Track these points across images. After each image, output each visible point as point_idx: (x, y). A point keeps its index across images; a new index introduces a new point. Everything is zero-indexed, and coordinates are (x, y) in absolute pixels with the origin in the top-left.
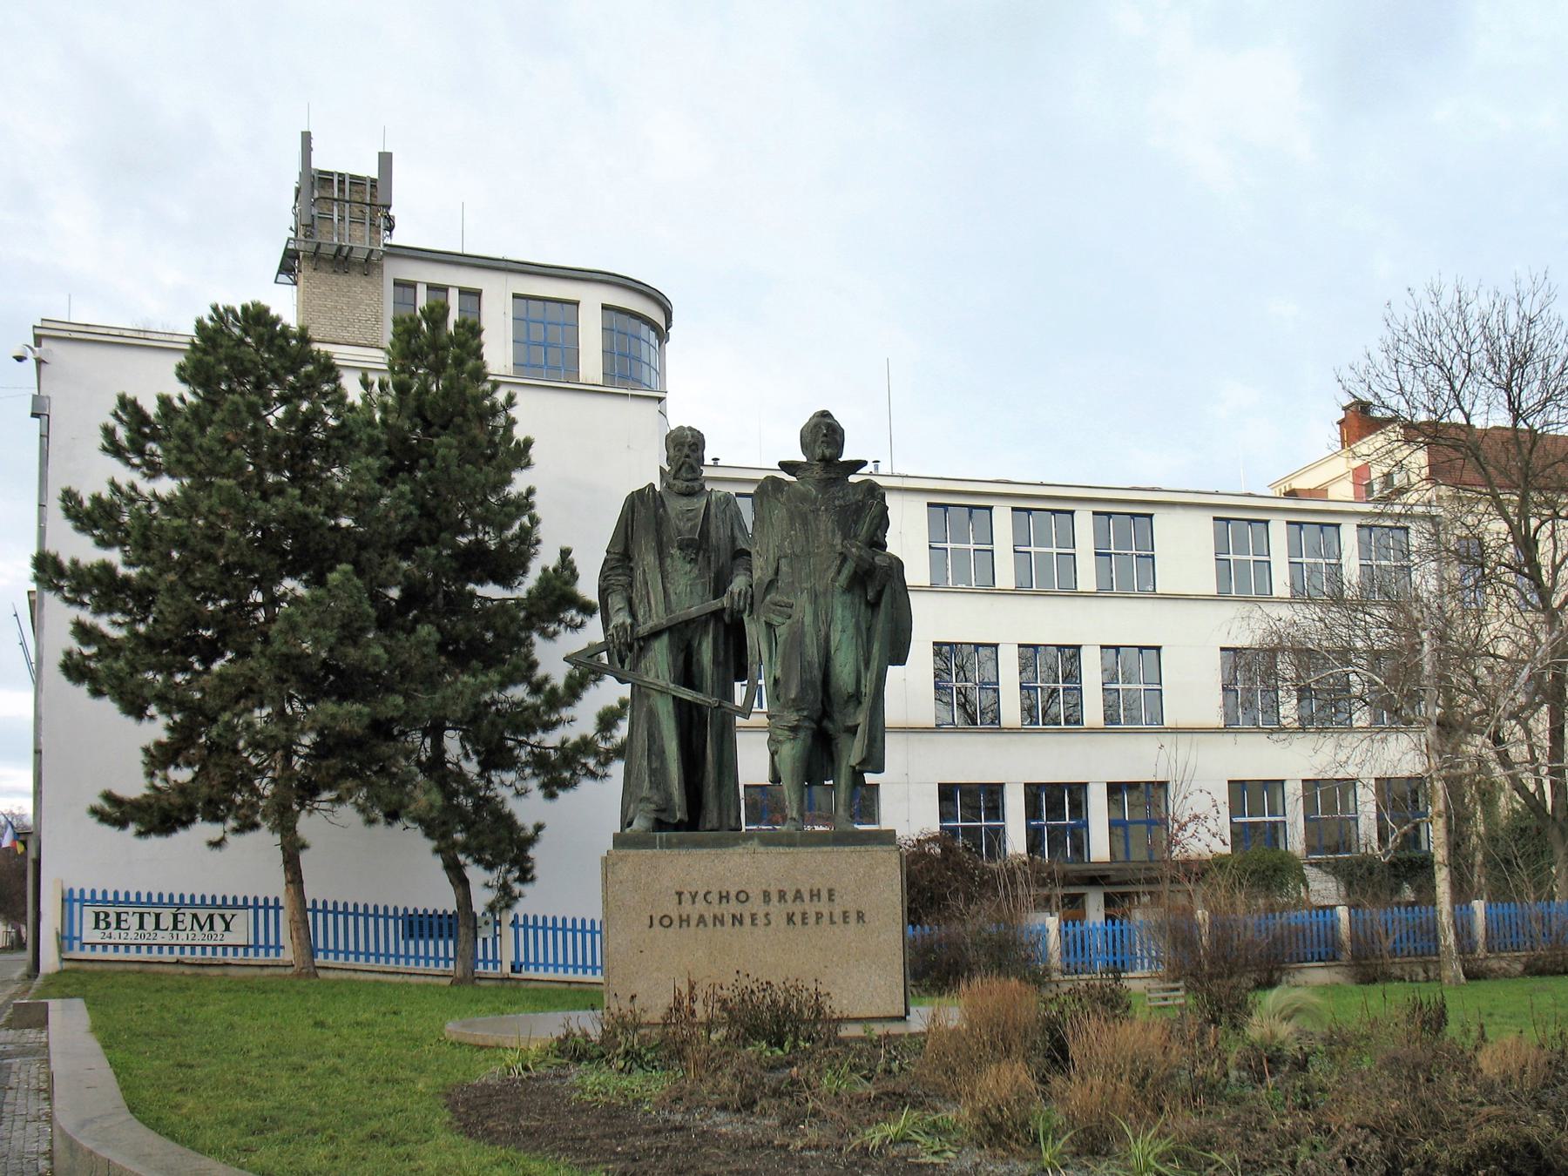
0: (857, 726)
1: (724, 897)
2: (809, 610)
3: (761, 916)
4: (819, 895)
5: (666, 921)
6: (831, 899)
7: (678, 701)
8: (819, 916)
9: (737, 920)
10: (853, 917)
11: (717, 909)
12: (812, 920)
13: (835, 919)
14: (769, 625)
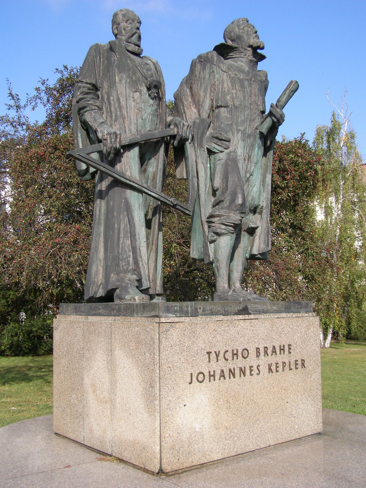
0: (257, 228)
2: (241, 144)
3: (255, 368)
4: (283, 350)
6: (290, 353)
9: (242, 371)
10: (299, 363)
11: (231, 365)
12: (280, 369)
13: (292, 367)
14: (210, 152)
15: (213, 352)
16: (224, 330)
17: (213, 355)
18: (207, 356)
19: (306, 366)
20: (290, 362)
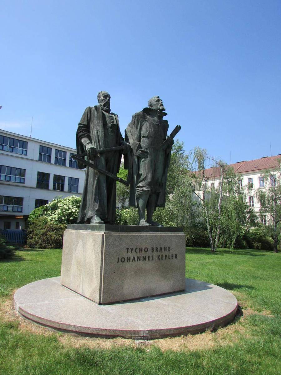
0: (160, 192)
1: (141, 250)
3: (151, 257)
5: (123, 260)
6: (169, 251)
7: (107, 178)
8: (166, 256)
10: (174, 256)
11: (139, 255)
12: (164, 258)
15: (130, 248)
16: (136, 239)
17: (130, 250)
18: (127, 250)
19: (177, 257)
20: (169, 255)
